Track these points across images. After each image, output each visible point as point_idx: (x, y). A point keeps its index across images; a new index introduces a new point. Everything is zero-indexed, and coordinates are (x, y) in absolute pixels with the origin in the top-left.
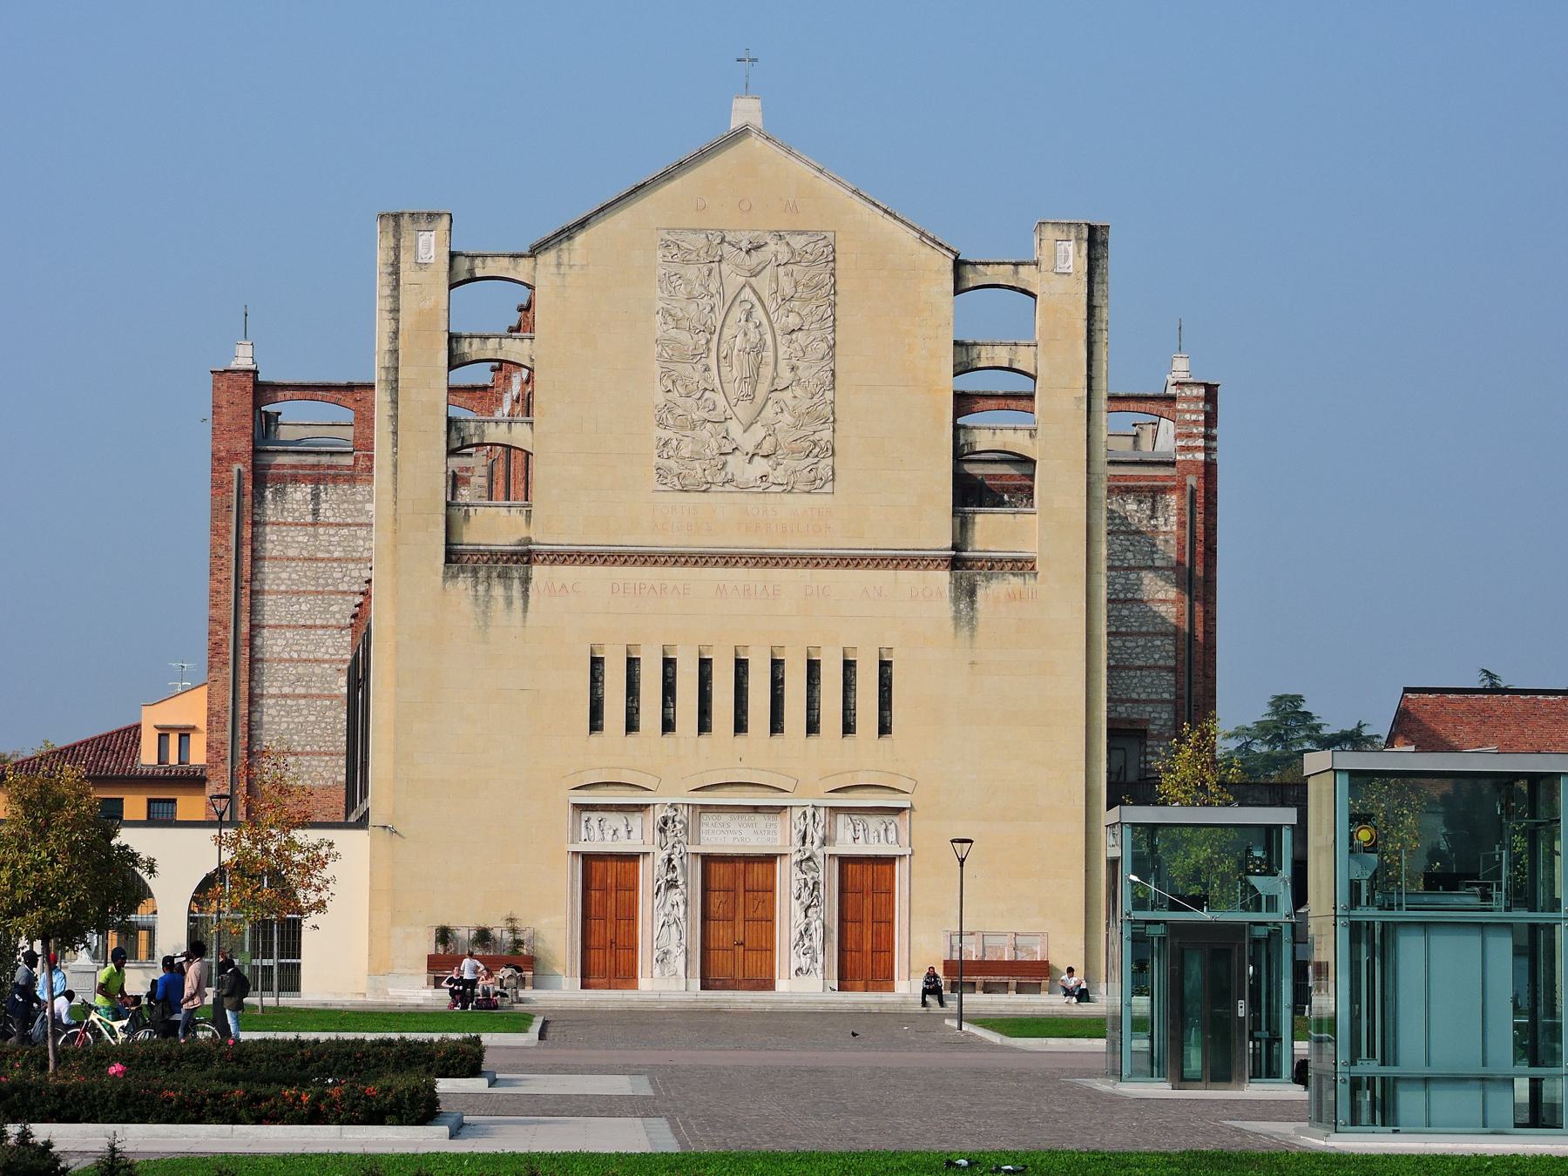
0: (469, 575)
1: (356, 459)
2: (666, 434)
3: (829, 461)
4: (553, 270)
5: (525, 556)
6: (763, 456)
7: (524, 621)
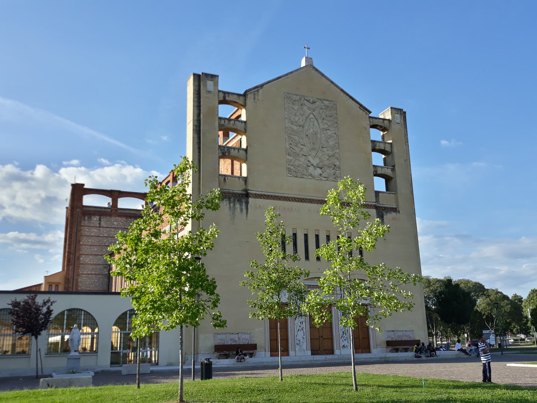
0: (228, 200)
1: (112, 210)
2: (291, 158)
3: (339, 171)
4: (253, 100)
5: (246, 195)
6: (320, 168)
7: (247, 217)
